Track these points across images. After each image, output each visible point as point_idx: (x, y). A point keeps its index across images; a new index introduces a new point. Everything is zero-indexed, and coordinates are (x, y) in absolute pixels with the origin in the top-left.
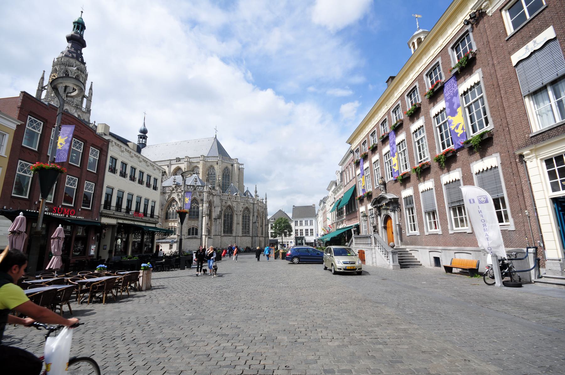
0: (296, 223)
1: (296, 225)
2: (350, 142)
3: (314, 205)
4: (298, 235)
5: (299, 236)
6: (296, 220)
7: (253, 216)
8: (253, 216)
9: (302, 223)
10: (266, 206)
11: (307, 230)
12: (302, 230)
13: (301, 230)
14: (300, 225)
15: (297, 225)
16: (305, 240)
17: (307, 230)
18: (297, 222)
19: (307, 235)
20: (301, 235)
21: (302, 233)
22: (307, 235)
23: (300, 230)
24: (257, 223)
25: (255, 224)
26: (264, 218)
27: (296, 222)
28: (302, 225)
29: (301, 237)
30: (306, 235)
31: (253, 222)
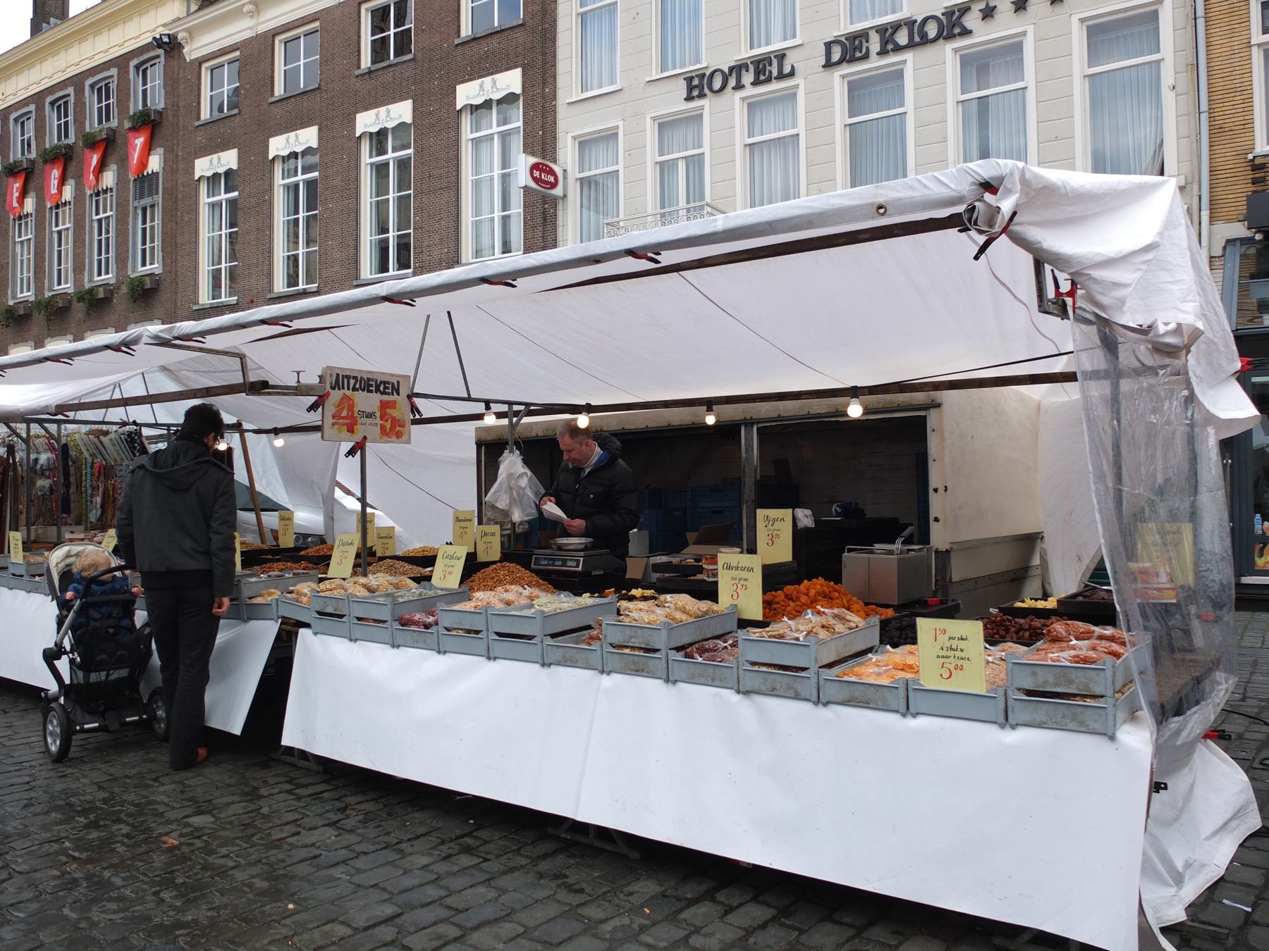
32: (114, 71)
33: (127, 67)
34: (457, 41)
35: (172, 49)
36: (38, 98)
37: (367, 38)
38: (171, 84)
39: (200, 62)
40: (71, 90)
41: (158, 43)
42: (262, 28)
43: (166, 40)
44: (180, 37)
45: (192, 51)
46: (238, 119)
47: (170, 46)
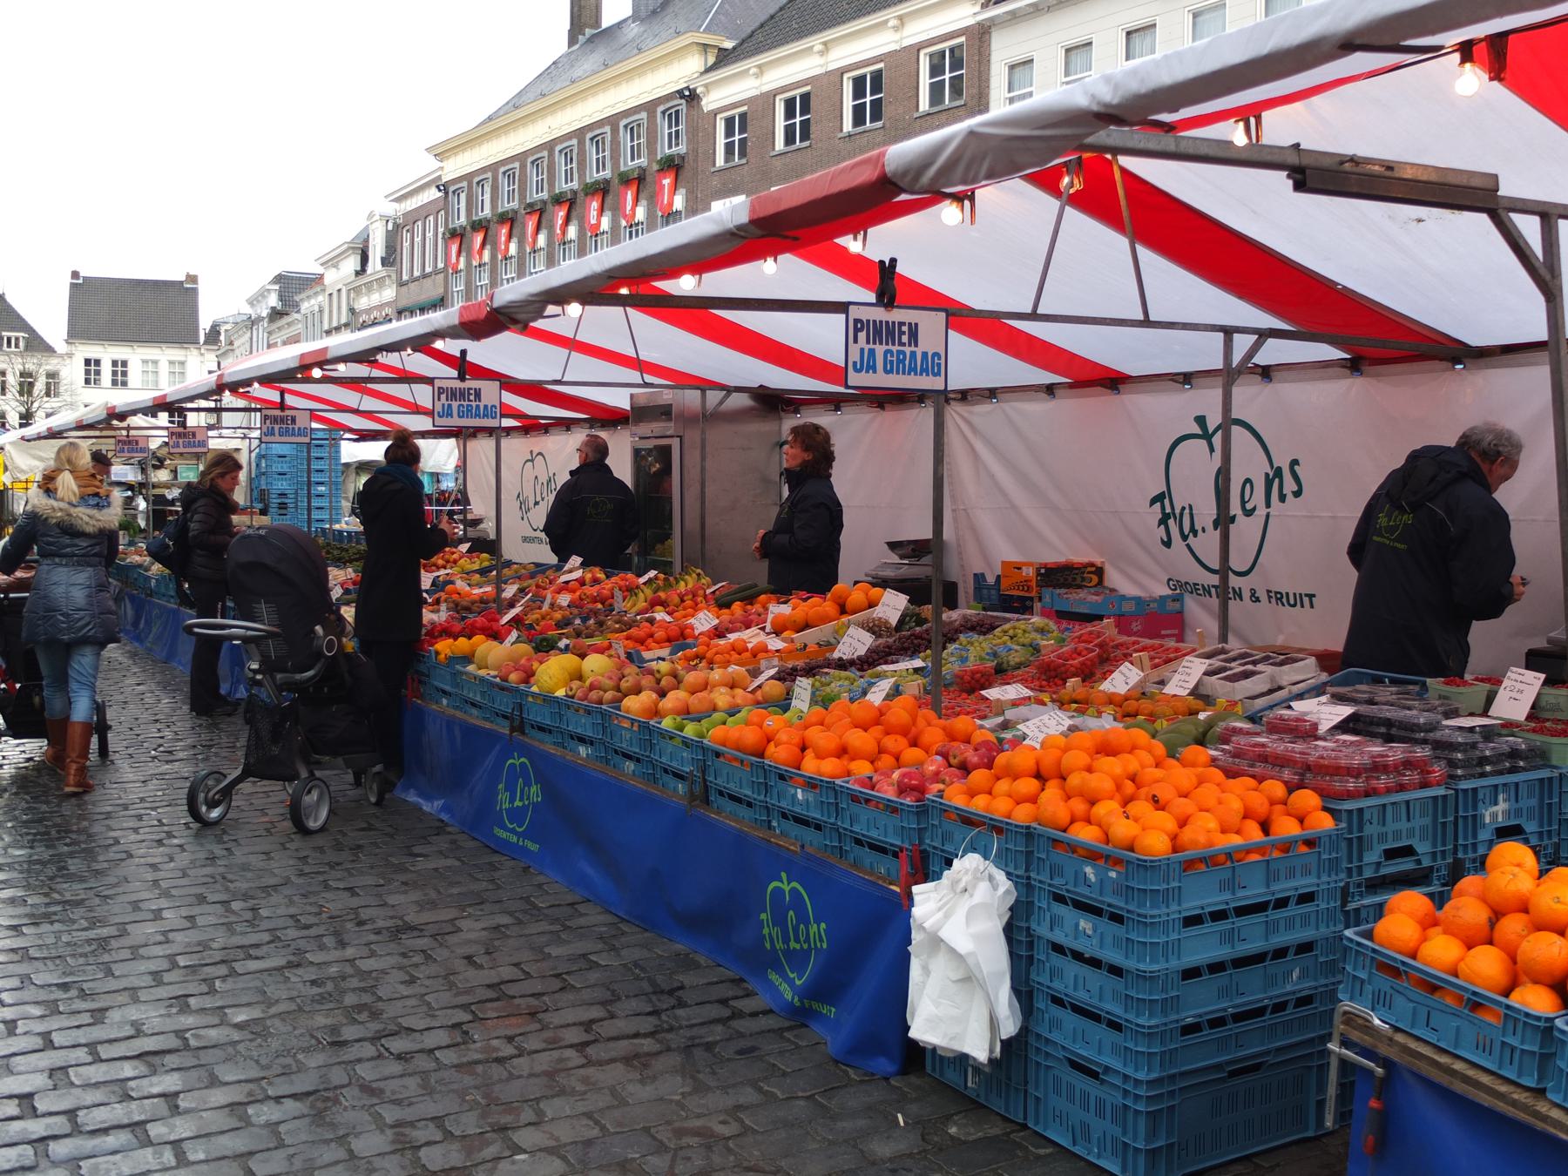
0: (87, 372)
1: (87, 381)
2: (442, 152)
3: (193, 279)
6: (89, 356)
9: (124, 374)
14: (114, 383)
18: (98, 362)
27: (87, 362)
28: (124, 384)
32: (644, 115)
33: (655, 112)
34: (916, 115)
35: (693, 100)
36: (580, 133)
37: (848, 103)
38: (693, 131)
39: (715, 113)
40: (607, 129)
41: (680, 93)
42: (765, 89)
43: (687, 93)
44: (698, 91)
45: (710, 102)
46: (746, 167)
47: (691, 97)
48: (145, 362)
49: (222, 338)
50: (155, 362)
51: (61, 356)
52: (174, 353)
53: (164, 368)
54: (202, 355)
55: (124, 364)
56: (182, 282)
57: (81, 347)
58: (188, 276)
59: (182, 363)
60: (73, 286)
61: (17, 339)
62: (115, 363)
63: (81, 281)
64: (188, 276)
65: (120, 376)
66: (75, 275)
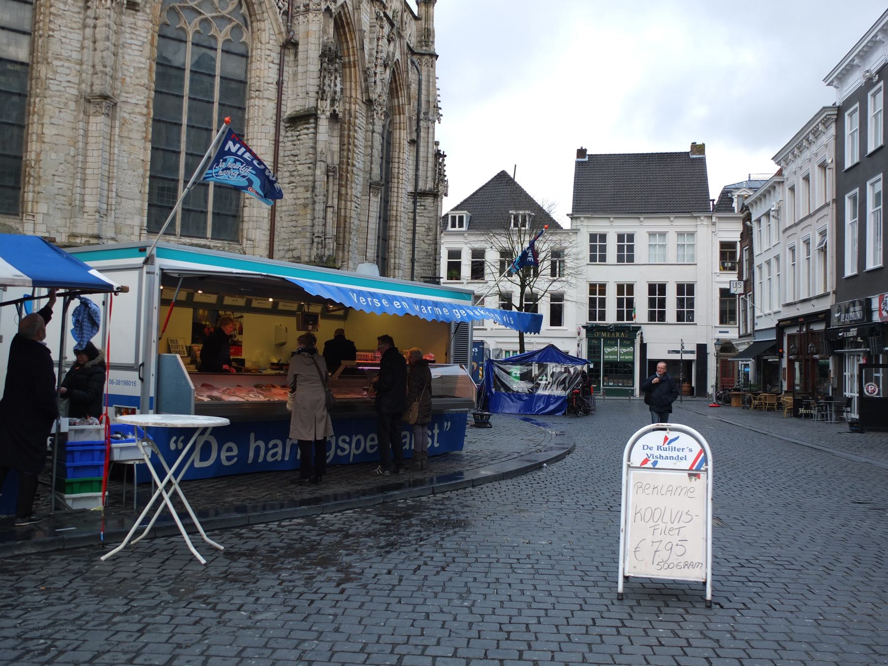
0: (593, 249)
1: (593, 259)
4: (602, 317)
5: (611, 318)
7: (290, 45)
8: (290, 45)
9: (631, 249)
10: (427, 35)
11: (657, 290)
12: (630, 288)
13: (626, 290)
14: (620, 259)
15: (603, 258)
16: (643, 347)
17: (657, 290)
18: (603, 237)
19: (657, 315)
20: (620, 316)
21: (626, 305)
22: (657, 315)
23: (620, 288)
24: (324, 123)
25: (305, 133)
26: (403, 136)
27: (593, 237)
28: (631, 259)
29: (618, 328)
30: (652, 317)
31: (289, 110)
48: (652, 235)
49: (735, 205)
50: (663, 235)
51: (567, 232)
52: (684, 224)
53: (672, 239)
54: (714, 224)
55: (631, 237)
56: (687, 154)
57: (586, 222)
58: (694, 145)
59: (692, 234)
60: (578, 164)
61: (524, 217)
62: (620, 238)
63: (586, 159)
64: (694, 145)
65: (626, 255)
66: (581, 153)
